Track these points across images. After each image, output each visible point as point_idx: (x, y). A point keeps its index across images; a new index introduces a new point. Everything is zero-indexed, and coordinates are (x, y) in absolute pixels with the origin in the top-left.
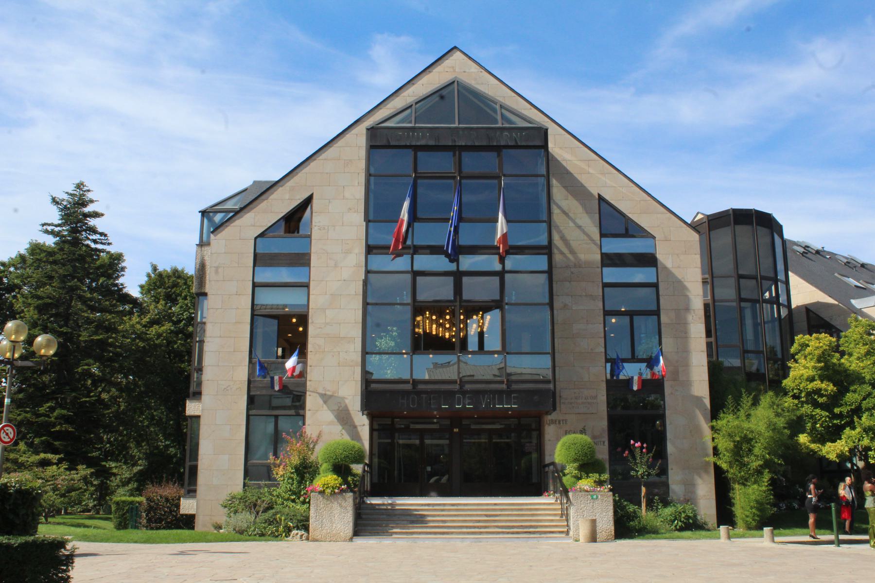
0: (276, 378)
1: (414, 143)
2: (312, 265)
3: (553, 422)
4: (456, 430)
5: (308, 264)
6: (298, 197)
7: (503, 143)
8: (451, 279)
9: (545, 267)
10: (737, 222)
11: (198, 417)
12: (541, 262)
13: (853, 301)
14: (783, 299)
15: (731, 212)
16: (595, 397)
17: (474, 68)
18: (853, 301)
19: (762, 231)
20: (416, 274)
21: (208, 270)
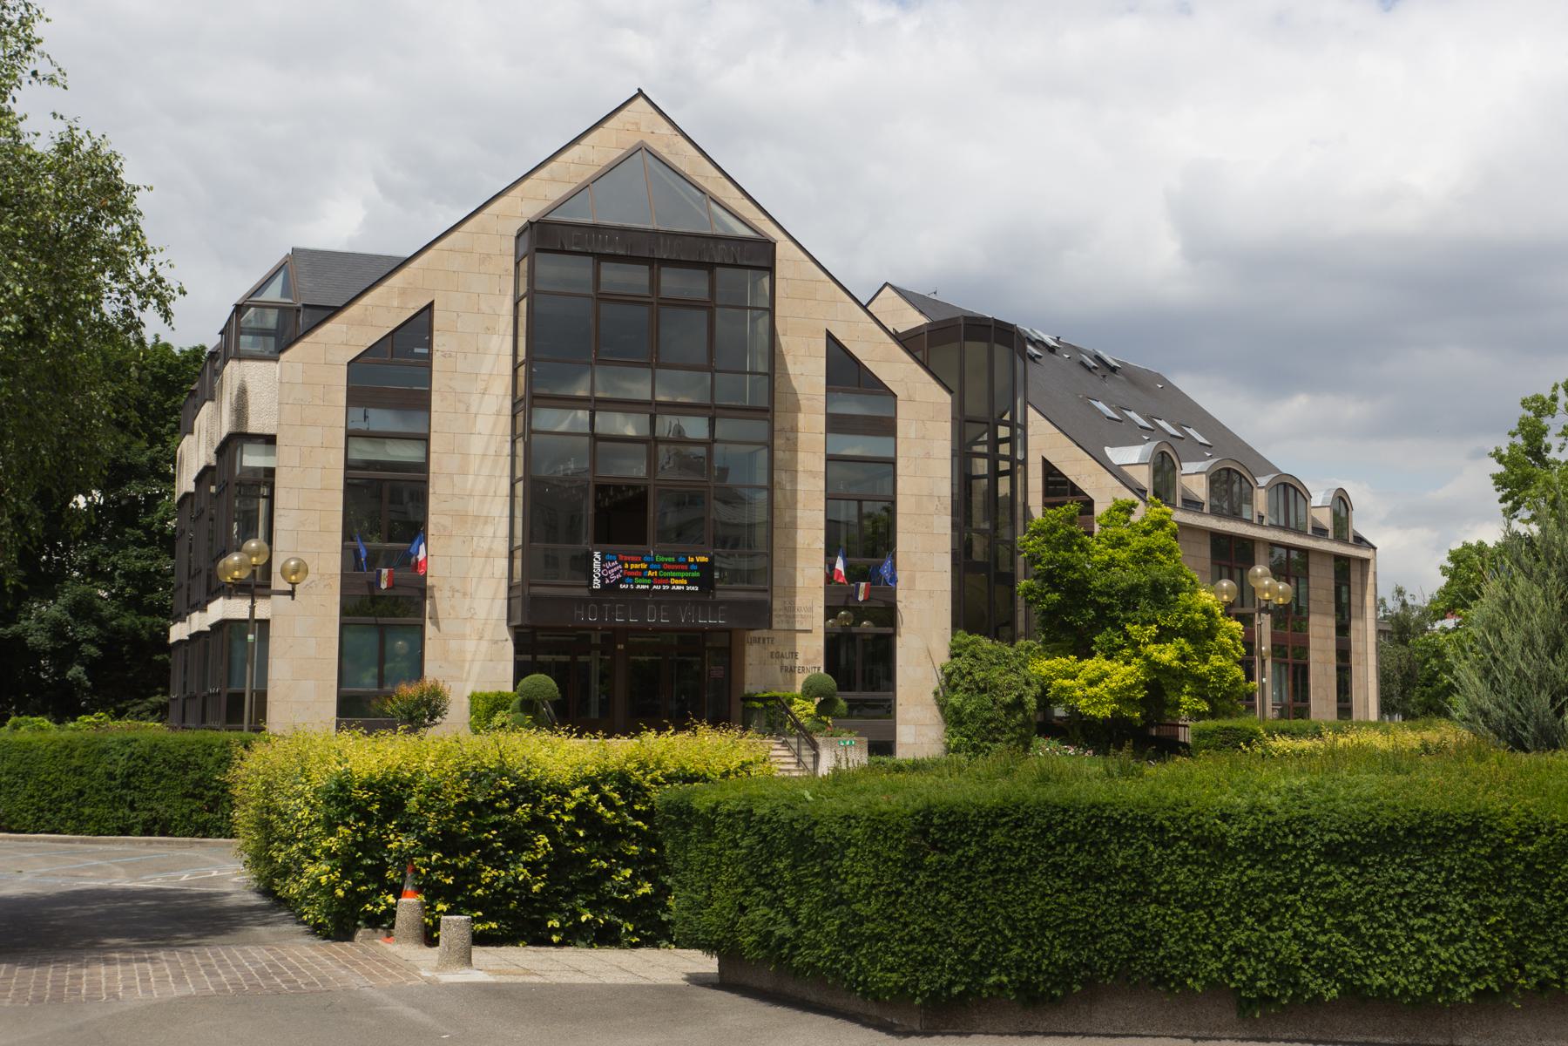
0: (385, 571)
1: (598, 250)
2: (433, 408)
3: (757, 640)
4: (620, 647)
5: (427, 407)
6: (411, 305)
7: (718, 260)
8: (643, 447)
9: (764, 437)
10: (970, 336)
11: (267, 621)
12: (757, 429)
13: (1107, 449)
14: (1020, 456)
15: (961, 321)
16: (811, 609)
17: (666, 128)
18: (1107, 449)
19: (1001, 352)
20: (595, 438)
21: (252, 398)
